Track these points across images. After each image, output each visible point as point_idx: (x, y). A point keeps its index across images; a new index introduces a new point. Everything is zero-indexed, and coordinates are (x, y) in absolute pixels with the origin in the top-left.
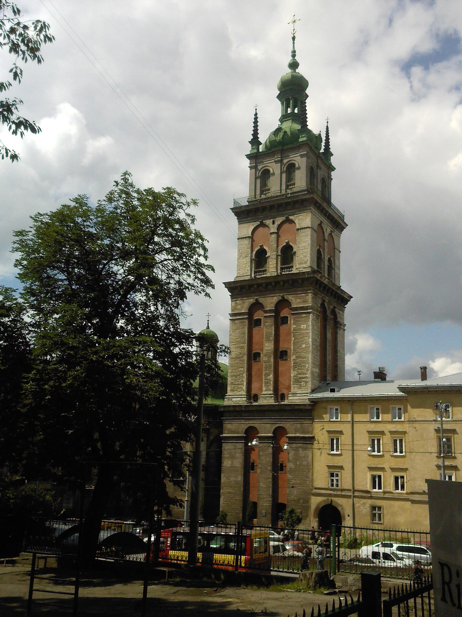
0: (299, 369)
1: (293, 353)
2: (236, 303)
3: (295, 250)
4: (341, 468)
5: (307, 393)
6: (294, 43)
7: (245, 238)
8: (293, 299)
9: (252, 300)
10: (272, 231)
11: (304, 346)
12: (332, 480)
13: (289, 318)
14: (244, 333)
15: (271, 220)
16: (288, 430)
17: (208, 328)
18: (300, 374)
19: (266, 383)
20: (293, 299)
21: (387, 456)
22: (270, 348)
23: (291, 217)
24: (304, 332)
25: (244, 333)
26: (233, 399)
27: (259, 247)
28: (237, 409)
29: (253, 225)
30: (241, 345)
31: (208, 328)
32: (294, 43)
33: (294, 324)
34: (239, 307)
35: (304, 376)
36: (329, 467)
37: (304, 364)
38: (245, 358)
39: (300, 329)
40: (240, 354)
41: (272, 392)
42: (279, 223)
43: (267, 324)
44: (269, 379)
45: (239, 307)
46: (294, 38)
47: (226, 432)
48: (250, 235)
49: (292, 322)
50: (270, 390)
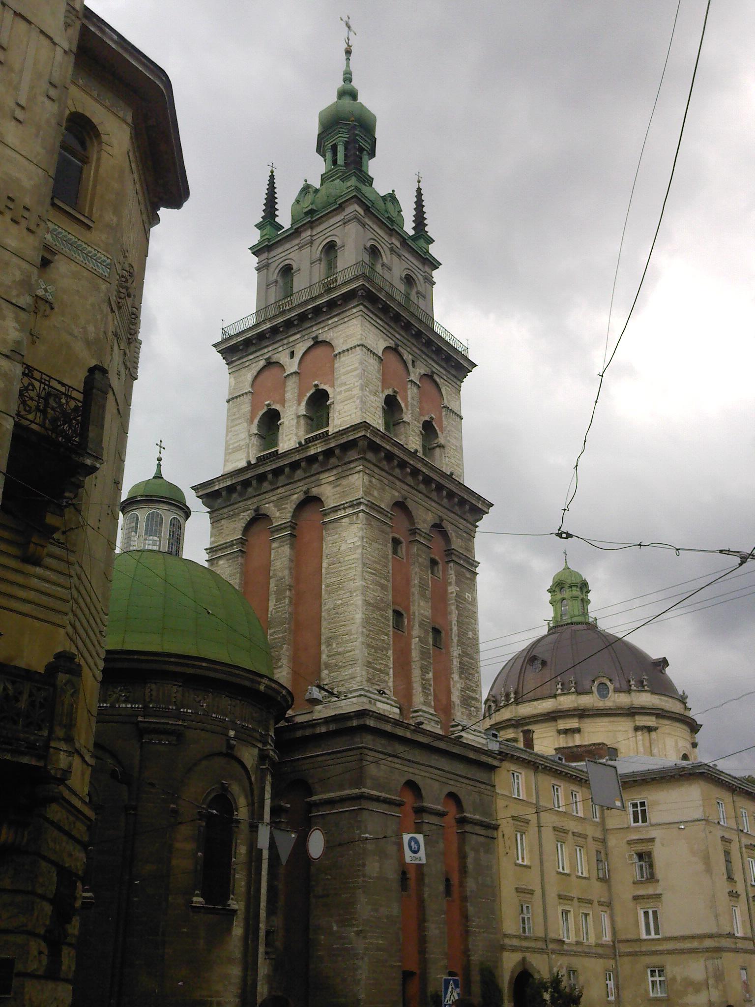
0: (467, 679)
1: (458, 641)
2: (370, 481)
3: (441, 440)
4: (531, 892)
5: (480, 732)
6: (348, 59)
7: (374, 353)
8: (453, 534)
9: (397, 494)
10: (412, 377)
11: (470, 635)
12: (523, 919)
13: (440, 567)
14: (386, 557)
15: (410, 357)
16: (465, 804)
17: (158, 476)
18: (468, 689)
19: (424, 687)
20: (453, 534)
21: (573, 878)
22: (426, 613)
23: (435, 377)
24: (470, 607)
25: (386, 557)
26: (379, 705)
27: (389, 392)
28: (400, 732)
29: (385, 340)
30: (383, 581)
31: (158, 476)
32: (348, 59)
33: (457, 584)
34: (376, 493)
35: (473, 695)
36: (518, 890)
37: (472, 672)
38: (390, 612)
39: (465, 599)
40: (382, 600)
41: (432, 711)
42: (423, 372)
43: (420, 560)
44: (428, 680)
45: (376, 493)
46: (348, 52)
47: (369, 782)
48: (380, 354)
49: (453, 578)
50: (430, 706)
